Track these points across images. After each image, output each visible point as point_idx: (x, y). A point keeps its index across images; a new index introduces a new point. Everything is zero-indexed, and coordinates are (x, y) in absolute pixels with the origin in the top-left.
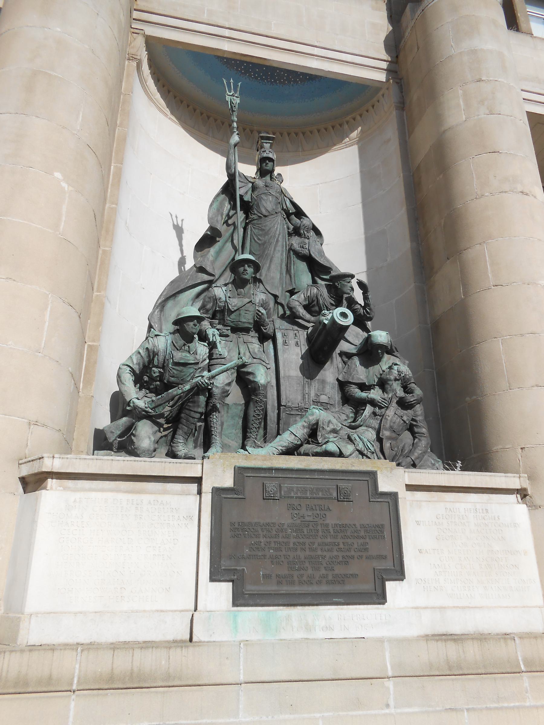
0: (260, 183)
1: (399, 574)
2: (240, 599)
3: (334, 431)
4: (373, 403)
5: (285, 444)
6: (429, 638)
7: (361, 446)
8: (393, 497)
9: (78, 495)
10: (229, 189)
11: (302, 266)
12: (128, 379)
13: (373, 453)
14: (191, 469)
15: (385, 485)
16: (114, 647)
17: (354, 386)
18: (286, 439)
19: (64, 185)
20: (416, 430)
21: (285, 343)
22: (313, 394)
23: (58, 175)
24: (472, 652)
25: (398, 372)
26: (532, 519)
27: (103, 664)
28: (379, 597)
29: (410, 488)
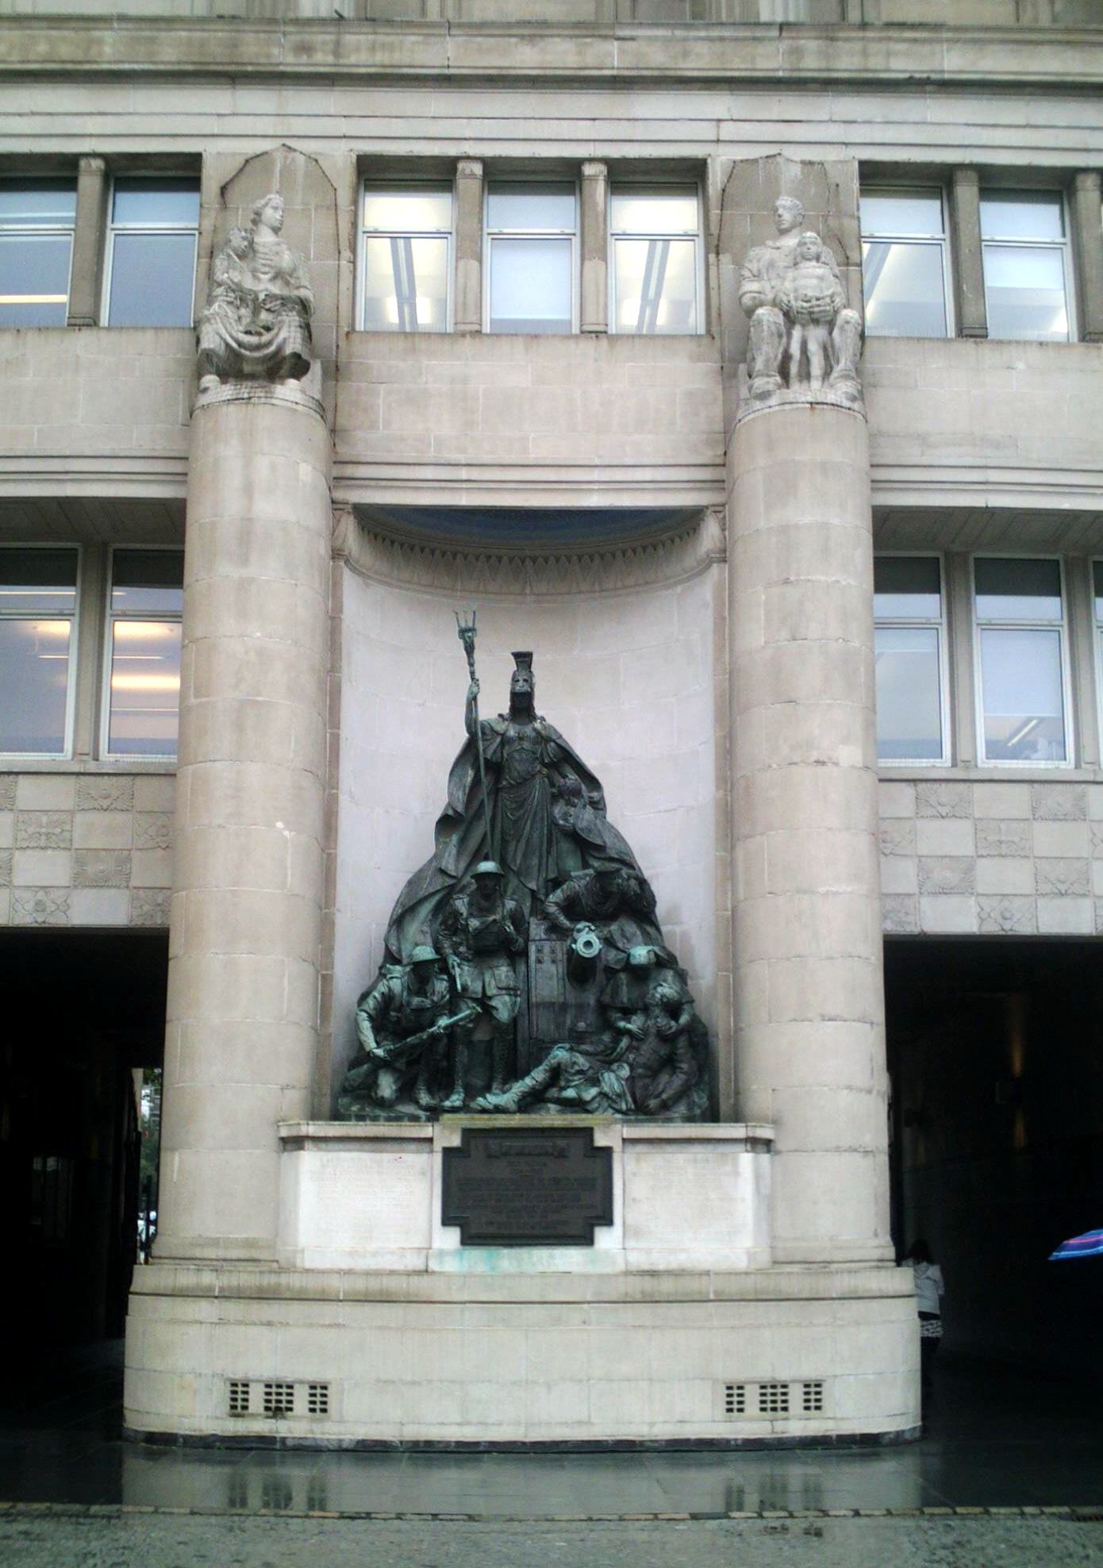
0: (512, 733)
1: (608, 1221)
2: (468, 1240)
3: (580, 1072)
4: (629, 1032)
6: (627, 1273)
7: (606, 1089)
8: (607, 1151)
9: (331, 1155)
10: (470, 748)
11: (565, 846)
12: (366, 1026)
13: (619, 1096)
14: (427, 1131)
15: (600, 1141)
16: (368, 1274)
19: (286, 833)
21: (539, 961)
22: (569, 1022)
23: (280, 825)
24: (667, 1286)
26: (772, 1163)
27: (360, 1284)
28: (587, 1240)
29: (625, 1141)
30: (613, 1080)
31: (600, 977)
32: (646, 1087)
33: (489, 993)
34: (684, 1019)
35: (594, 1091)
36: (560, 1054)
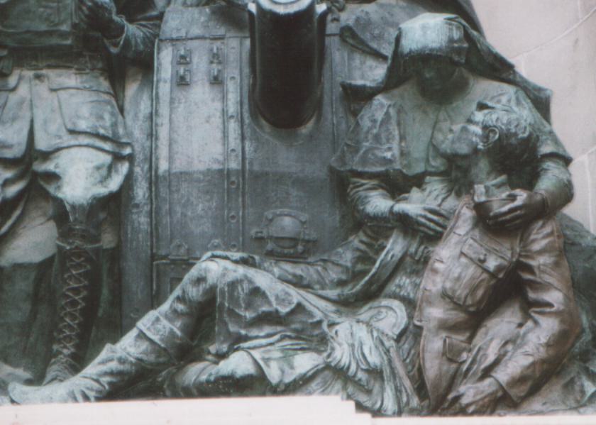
4: (406, 224)
5: (121, 367)
7: (342, 355)
13: (376, 373)
17: (370, 183)
18: (128, 348)
20: (532, 295)
25: (485, 128)
30: (358, 338)
31: (333, 113)
32: (450, 354)
33: (42, 144)
34: (546, 184)
35: (305, 362)
36: (216, 269)
